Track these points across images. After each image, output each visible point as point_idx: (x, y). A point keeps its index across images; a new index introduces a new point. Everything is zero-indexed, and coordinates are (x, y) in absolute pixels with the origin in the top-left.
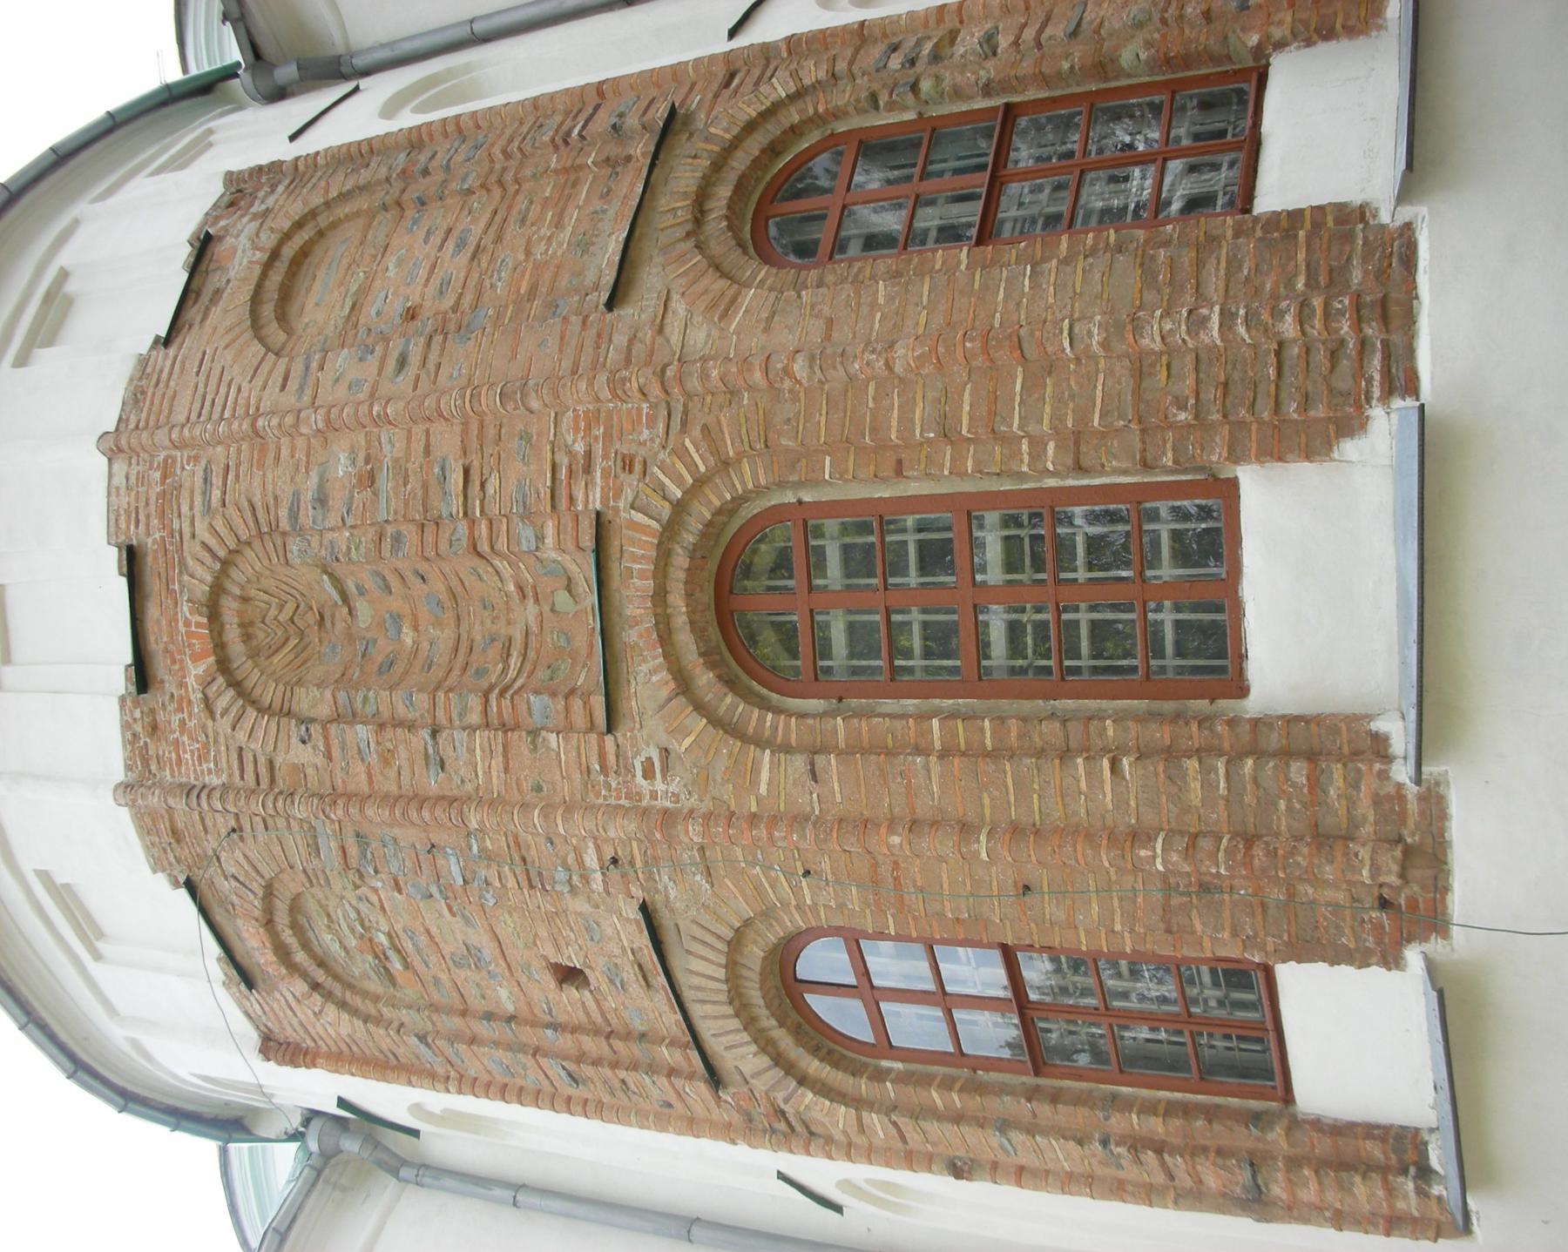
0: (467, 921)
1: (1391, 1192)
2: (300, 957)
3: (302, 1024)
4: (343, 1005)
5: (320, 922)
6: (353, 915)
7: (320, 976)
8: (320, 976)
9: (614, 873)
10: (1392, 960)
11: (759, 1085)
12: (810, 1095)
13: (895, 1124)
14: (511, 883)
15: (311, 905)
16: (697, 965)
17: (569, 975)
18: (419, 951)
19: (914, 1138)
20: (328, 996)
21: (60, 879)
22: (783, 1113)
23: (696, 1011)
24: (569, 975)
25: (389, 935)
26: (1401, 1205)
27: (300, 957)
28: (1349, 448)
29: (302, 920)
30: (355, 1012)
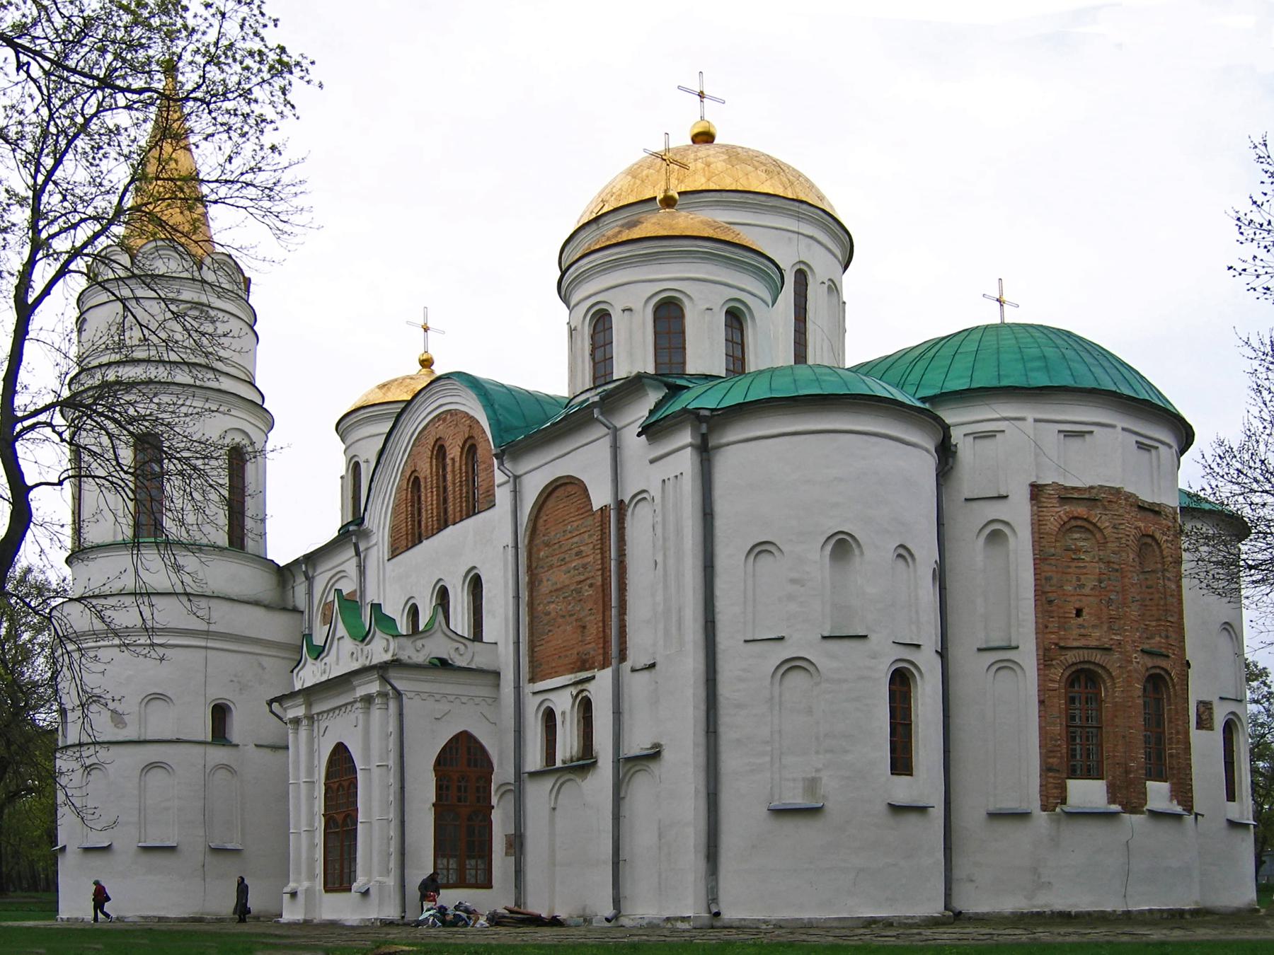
0: (1092, 589)
1: (1057, 798)
2: (1074, 523)
3: (1047, 507)
5: (1083, 536)
6: (1089, 550)
7: (1068, 526)
8: (1068, 526)
9: (1117, 643)
11: (1062, 658)
13: (1056, 690)
15: (1089, 536)
16: (1099, 656)
17: (1079, 613)
18: (1080, 567)
19: (1051, 693)
20: (1062, 526)
21: (1087, 437)
22: (1052, 661)
23: (1086, 651)
24: (1079, 613)
27: (1074, 523)
29: (1083, 530)
30: (1058, 533)
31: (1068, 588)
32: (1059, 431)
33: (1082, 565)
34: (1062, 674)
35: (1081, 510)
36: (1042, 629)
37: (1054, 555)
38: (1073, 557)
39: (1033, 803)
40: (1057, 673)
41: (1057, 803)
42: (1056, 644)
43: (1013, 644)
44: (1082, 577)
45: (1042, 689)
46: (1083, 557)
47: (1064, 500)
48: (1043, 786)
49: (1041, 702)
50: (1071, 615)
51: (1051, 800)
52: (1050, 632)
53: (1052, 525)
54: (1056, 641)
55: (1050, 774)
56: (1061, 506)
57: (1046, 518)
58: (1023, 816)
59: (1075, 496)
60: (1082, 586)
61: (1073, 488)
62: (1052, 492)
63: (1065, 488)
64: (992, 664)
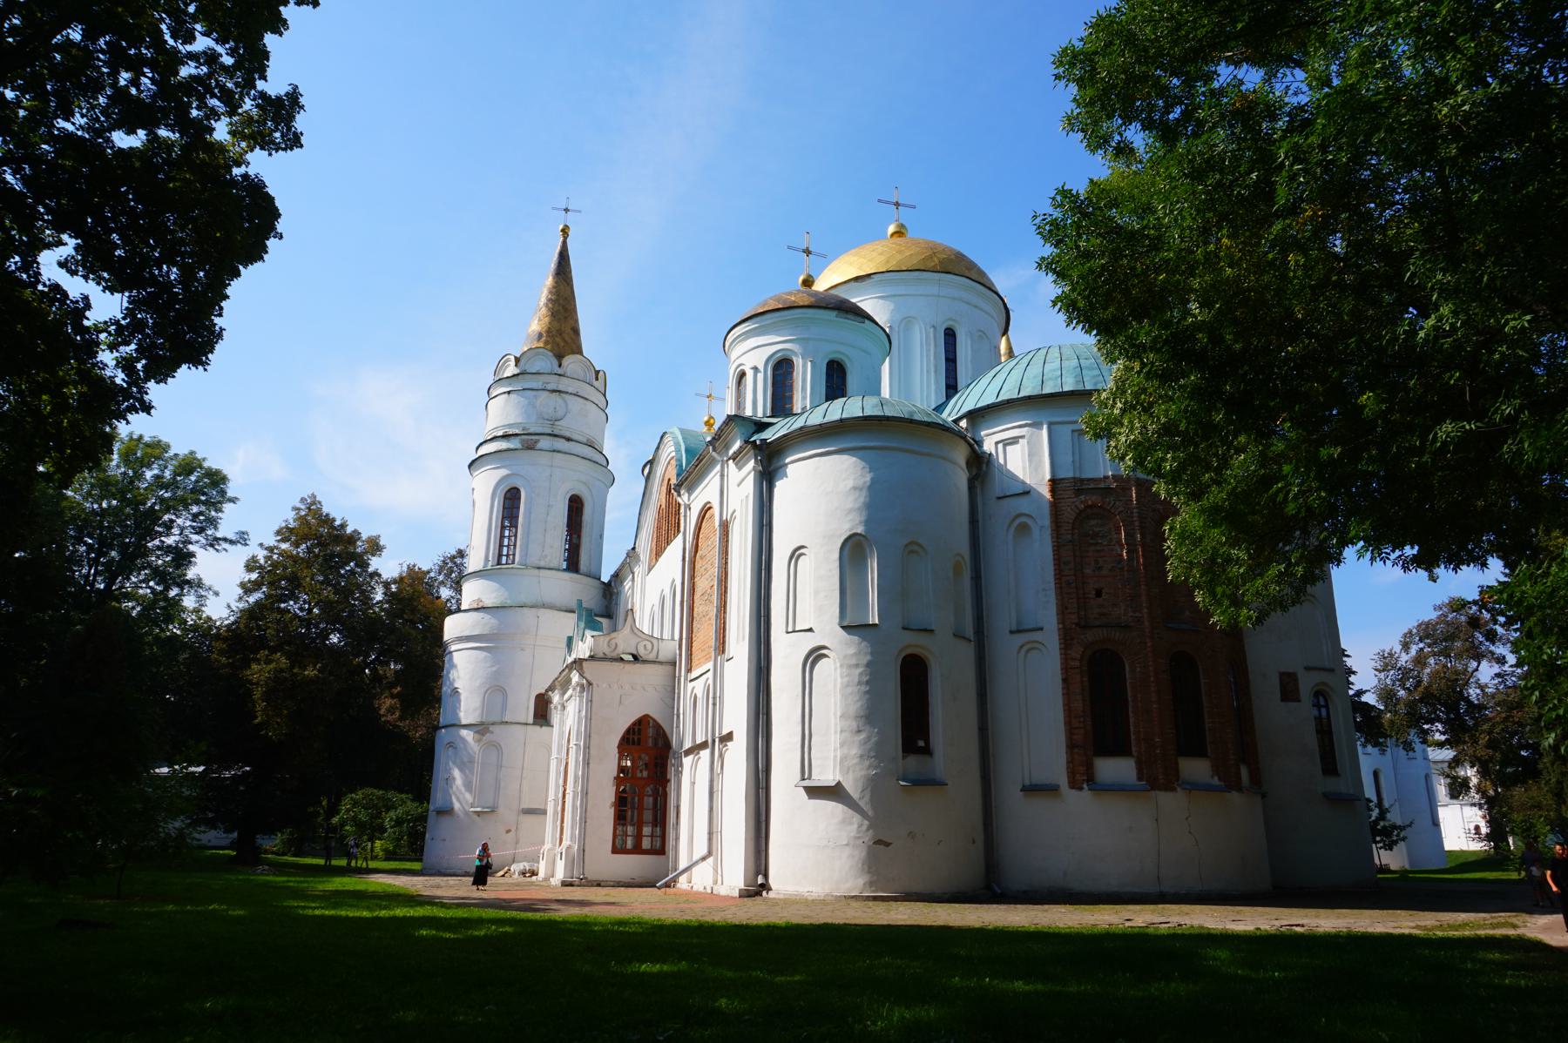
0: (1110, 570)
3: (1063, 498)
4: (1076, 518)
10: (1140, 779)
12: (1082, 650)
14: (1128, 591)
17: (1099, 593)
18: (1098, 551)
24: (1099, 593)
25: (1101, 543)
26: (1078, 775)
28: (1216, 778)
31: (1088, 571)
32: (1073, 431)
33: (1099, 548)
34: (1083, 652)
35: (1093, 499)
36: (1063, 611)
37: (1071, 541)
38: (1092, 541)
39: (1063, 780)
40: (1076, 652)
41: (1084, 780)
42: (1077, 624)
43: (1040, 625)
44: (1100, 559)
45: (1066, 669)
46: (1100, 541)
47: (1078, 492)
48: (1070, 761)
49: (1065, 680)
50: (1090, 596)
51: (1078, 777)
52: (1070, 613)
53: (1069, 514)
54: (1076, 621)
55: (1076, 750)
56: (1076, 497)
57: (1063, 508)
58: (1051, 790)
59: (1092, 486)
60: (1100, 568)
61: (1089, 480)
62: (1068, 485)
63: (1082, 480)
64: (1021, 647)
